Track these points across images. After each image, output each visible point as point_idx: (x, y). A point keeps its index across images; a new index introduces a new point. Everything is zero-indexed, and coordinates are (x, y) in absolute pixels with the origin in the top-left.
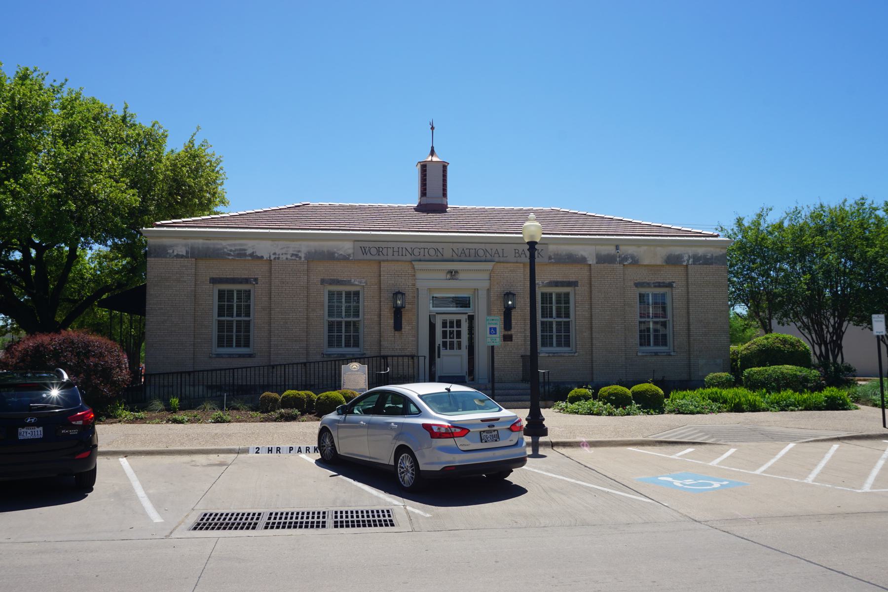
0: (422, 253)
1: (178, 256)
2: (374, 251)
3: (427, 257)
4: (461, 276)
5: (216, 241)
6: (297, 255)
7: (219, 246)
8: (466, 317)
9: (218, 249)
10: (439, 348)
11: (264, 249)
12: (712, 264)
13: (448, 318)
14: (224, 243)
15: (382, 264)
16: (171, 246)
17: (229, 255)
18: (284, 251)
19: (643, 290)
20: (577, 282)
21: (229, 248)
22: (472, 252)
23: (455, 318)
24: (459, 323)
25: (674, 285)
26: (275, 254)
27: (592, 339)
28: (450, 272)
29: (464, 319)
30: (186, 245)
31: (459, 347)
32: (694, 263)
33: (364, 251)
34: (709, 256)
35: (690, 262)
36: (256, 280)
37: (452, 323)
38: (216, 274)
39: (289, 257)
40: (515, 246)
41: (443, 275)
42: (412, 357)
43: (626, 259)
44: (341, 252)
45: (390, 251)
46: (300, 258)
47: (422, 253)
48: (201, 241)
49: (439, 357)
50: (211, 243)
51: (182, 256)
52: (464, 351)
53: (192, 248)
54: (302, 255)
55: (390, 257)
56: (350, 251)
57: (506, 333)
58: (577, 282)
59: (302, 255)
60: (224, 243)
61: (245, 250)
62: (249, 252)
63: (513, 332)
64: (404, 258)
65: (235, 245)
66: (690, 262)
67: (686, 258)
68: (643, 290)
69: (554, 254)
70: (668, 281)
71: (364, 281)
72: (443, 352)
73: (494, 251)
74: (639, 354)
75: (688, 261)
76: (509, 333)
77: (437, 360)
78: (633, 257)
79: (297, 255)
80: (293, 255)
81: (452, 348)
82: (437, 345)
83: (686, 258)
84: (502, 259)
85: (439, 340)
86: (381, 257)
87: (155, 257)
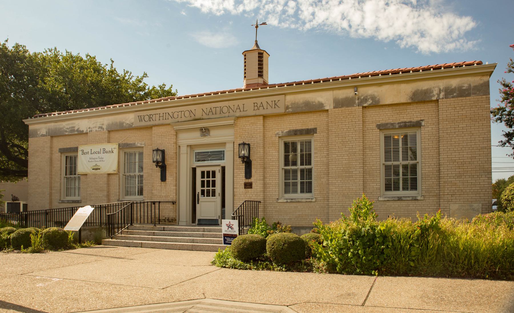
0: (180, 116)
2: (147, 118)
3: (184, 119)
4: (213, 133)
6: (101, 128)
7: (61, 126)
8: (219, 168)
9: (61, 129)
10: (198, 195)
12: (469, 95)
13: (206, 169)
17: (66, 131)
18: (94, 126)
19: (388, 132)
20: (316, 129)
22: (218, 110)
23: (211, 169)
24: (214, 173)
25: (423, 123)
26: (89, 128)
27: (328, 184)
28: (201, 129)
29: (218, 170)
31: (214, 195)
32: (446, 97)
34: (466, 86)
35: (441, 96)
37: (208, 172)
39: (97, 129)
40: (254, 100)
41: (198, 134)
42: (174, 203)
43: (366, 100)
44: (128, 122)
45: (158, 116)
46: (103, 129)
47: (180, 116)
48: (53, 124)
49: (198, 203)
52: (218, 198)
53: (49, 129)
54: (104, 127)
55: (157, 122)
56: (133, 121)
58: (316, 129)
59: (104, 127)
61: (74, 127)
62: (76, 129)
63: (252, 180)
64: (167, 122)
66: (441, 96)
67: (435, 92)
68: (388, 132)
69: (292, 104)
70: (415, 119)
71: (143, 143)
72: (201, 198)
73: (236, 106)
74: (381, 199)
75: (439, 95)
76: (250, 181)
77: (197, 205)
78: (373, 98)
79: (101, 128)
80: (99, 127)
81: (208, 195)
82: (197, 193)
83: (435, 92)
84: (243, 114)
85: (199, 189)
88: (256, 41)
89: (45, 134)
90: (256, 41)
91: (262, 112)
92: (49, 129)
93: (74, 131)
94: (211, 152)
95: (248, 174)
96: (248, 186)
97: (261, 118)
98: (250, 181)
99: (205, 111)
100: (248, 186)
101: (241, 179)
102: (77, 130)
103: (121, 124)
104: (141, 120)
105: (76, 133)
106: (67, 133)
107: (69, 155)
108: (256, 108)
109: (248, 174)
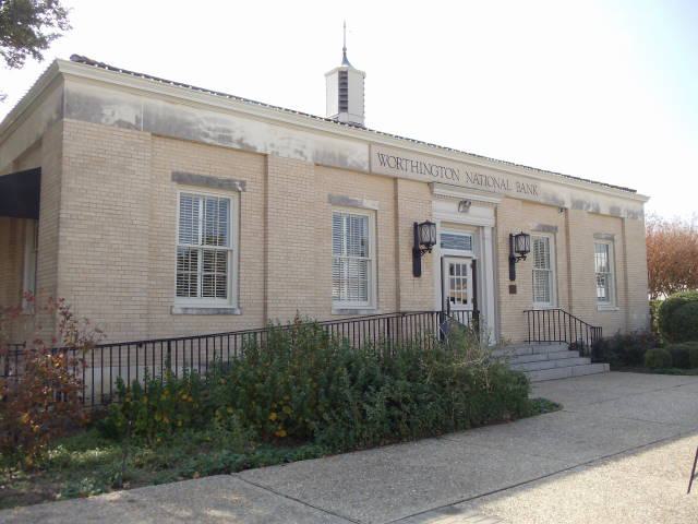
1: (120, 123)
4: (473, 209)
5: (185, 108)
7: (190, 118)
9: (189, 124)
11: (259, 136)
13: (455, 261)
14: (199, 114)
15: (400, 182)
16: (110, 103)
17: (207, 136)
30: (136, 106)
33: (383, 160)
36: (243, 184)
38: (185, 167)
39: (293, 156)
41: (454, 207)
44: (355, 158)
48: (161, 103)
50: (179, 110)
51: (129, 126)
53: (147, 114)
60: (199, 114)
61: (229, 131)
65: (214, 120)
86: (399, 173)
87: (78, 118)
89: (133, 122)
92: (147, 114)
93: (229, 139)
94: (458, 236)
96: (513, 290)
100: (513, 290)
102: (240, 142)
103: (343, 158)
105: (237, 147)
106: (208, 141)
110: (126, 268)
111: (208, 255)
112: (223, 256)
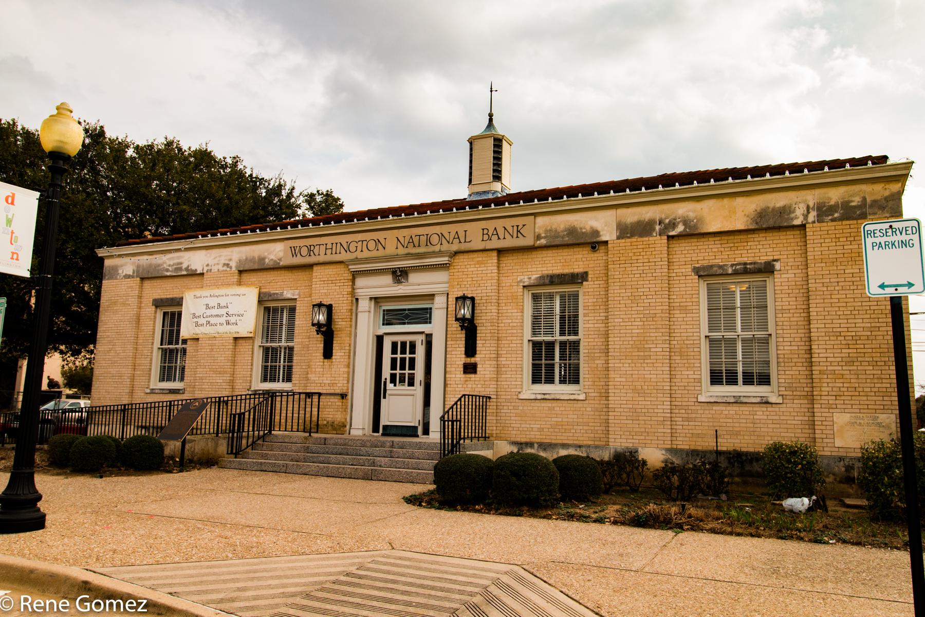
0: (359, 249)
2: (304, 251)
4: (413, 277)
6: (228, 265)
8: (423, 337)
9: (159, 265)
10: (385, 383)
17: (167, 270)
18: (216, 261)
20: (586, 273)
21: (168, 263)
22: (423, 239)
23: (408, 338)
24: (413, 346)
25: (778, 266)
26: (208, 265)
27: (607, 369)
29: (419, 340)
31: (411, 384)
32: (820, 219)
34: (856, 201)
37: (404, 344)
39: (221, 268)
40: (483, 224)
41: (388, 279)
42: (343, 396)
43: (673, 225)
44: (272, 257)
45: (323, 248)
46: (231, 268)
47: (359, 249)
49: (385, 397)
52: (419, 389)
55: (322, 258)
56: (281, 254)
57: (469, 360)
58: (586, 273)
59: (233, 264)
61: (181, 263)
63: (477, 359)
67: (800, 211)
70: (764, 259)
72: (390, 386)
75: (806, 217)
76: (473, 360)
77: (383, 400)
78: (686, 222)
82: (383, 380)
83: (800, 211)
84: (463, 247)
85: (386, 372)
88: (491, 115)
90: (491, 115)
91: (496, 244)
92: (138, 266)
93: (181, 269)
94: (409, 310)
95: (471, 350)
96: (470, 369)
97: (495, 254)
98: (473, 360)
99: (402, 240)
100: (470, 369)
101: (459, 357)
102: (187, 269)
103: (262, 260)
104: (294, 254)
105: (185, 273)
106: (168, 274)
107: (170, 310)
108: (486, 237)
109: (471, 350)
110: (833, 359)
111: (563, 344)
112: (575, 345)
